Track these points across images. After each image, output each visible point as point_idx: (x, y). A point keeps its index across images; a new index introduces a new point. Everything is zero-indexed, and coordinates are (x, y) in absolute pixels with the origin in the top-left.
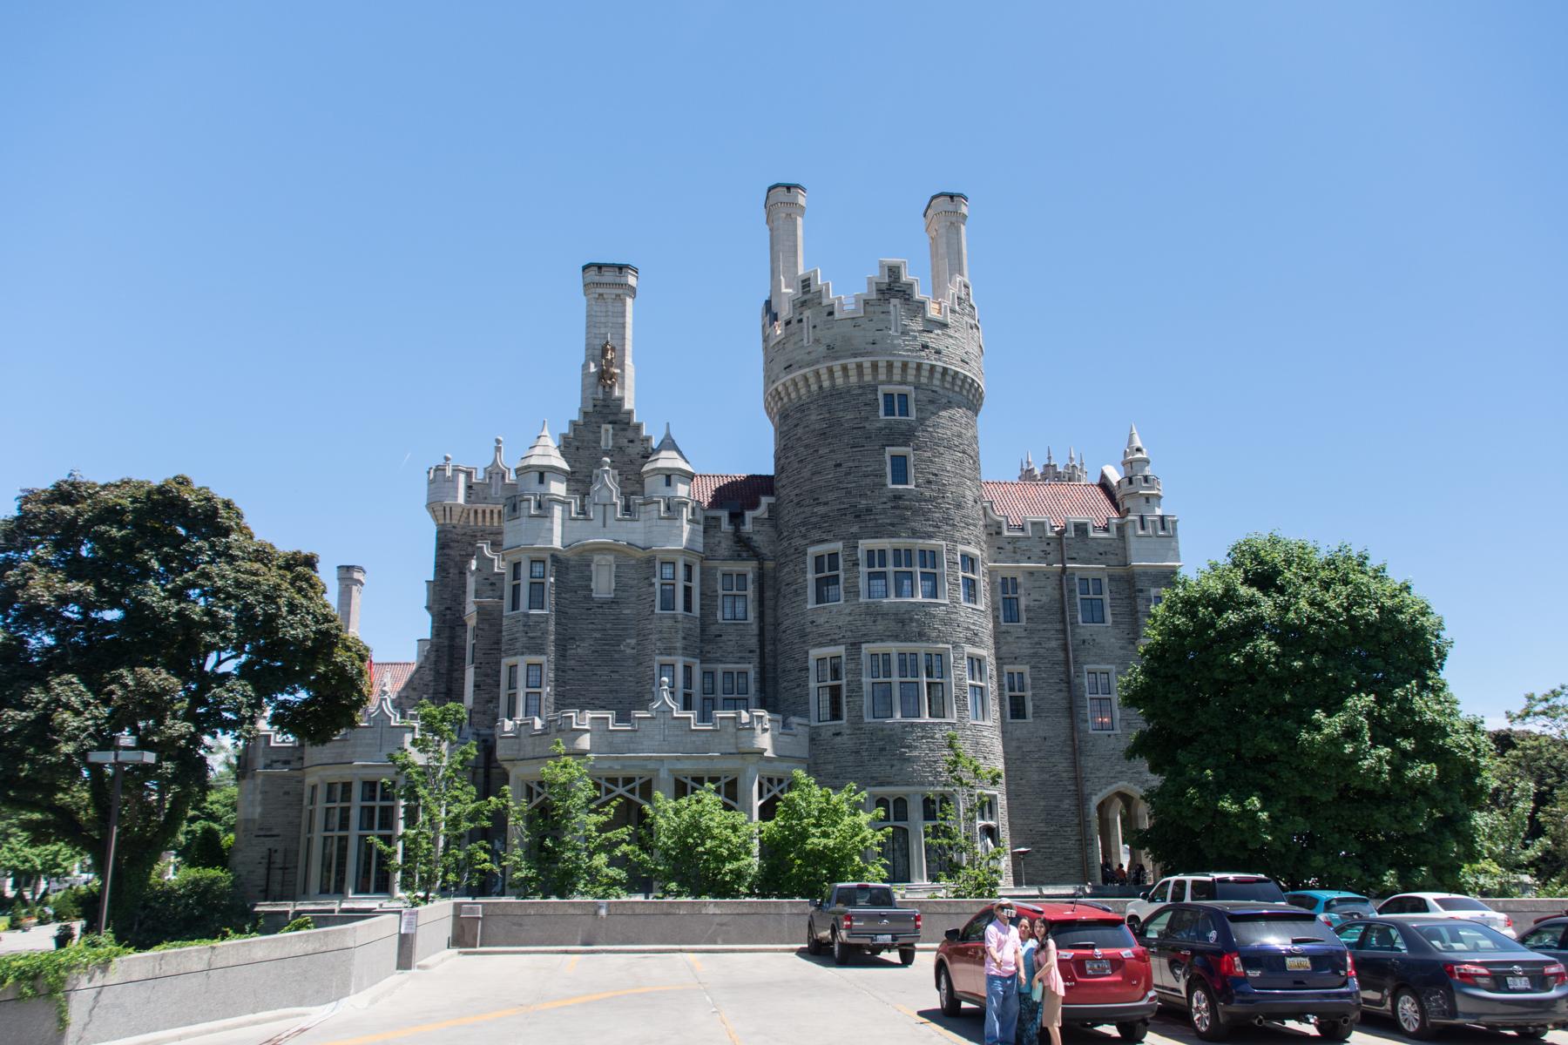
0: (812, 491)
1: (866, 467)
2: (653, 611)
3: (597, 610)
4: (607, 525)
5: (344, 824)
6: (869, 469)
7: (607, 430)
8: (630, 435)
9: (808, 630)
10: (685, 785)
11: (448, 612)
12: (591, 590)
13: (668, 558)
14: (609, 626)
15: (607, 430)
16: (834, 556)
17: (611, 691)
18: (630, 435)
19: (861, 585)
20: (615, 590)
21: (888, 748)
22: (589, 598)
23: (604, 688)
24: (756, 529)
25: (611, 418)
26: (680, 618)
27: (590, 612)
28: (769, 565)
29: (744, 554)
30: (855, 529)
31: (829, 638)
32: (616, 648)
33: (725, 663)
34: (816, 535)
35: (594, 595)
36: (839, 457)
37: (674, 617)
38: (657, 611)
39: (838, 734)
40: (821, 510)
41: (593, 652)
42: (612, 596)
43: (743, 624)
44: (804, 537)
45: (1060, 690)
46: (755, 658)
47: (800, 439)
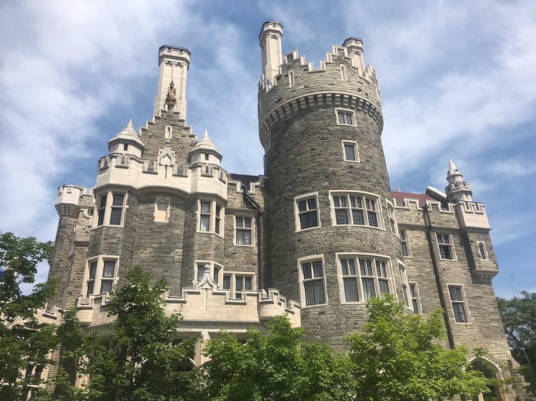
0: (296, 165)
4: (167, 177)
6: (278, 213)
7: (169, 129)
11: (61, 262)
14: (164, 240)
16: (312, 201)
19: (332, 216)
21: (359, 322)
30: (326, 184)
32: (169, 255)
36: (313, 145)
39: (323, 313)
43: (249, 248)
45: (436, 297)
46: (256, 268)
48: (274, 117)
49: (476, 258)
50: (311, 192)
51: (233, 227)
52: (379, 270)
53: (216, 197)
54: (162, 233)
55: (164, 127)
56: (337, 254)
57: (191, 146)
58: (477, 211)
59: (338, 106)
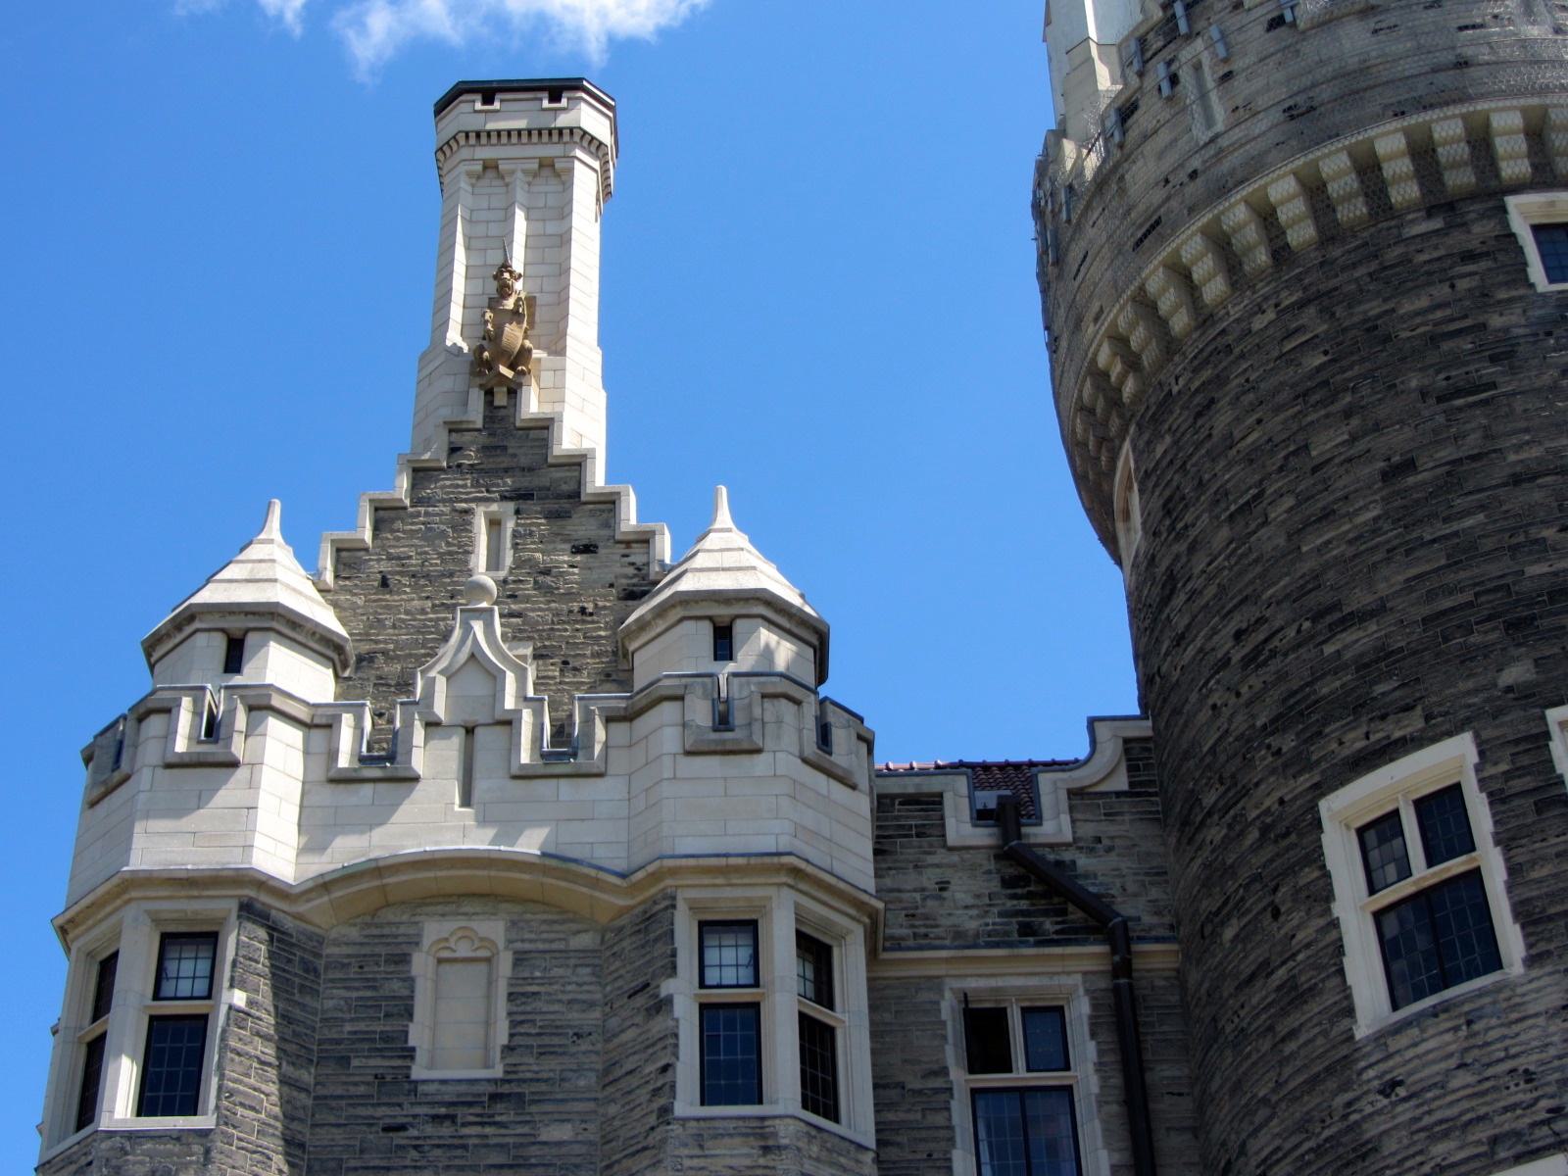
1: (1518, 448)
2: (665, 1111)
7: (494, 524)
8: (583, 528)
9: (1371, 1131)
12: (410, 1053)
13: (730, 900)
18: (583, 528)
20: (508, 1049)
22: (398, 1083)
24: (1088, 830)
26: (786, 1133)
27: (399, 1138)
28: (1156, 958)
29: (1049, 925)
30: (1516, 673)
31: (1483, 1133)
35: (418, 1072)
36: (1398, 440)
37: (762, 1136)
38: (687, 1102)
40: (1358, 640)
42: (498, 1072)
44: (1298, 763)
47: (1230, 442)
48: (1134, 345)
51: (944, 1071)
55: (466, 512)
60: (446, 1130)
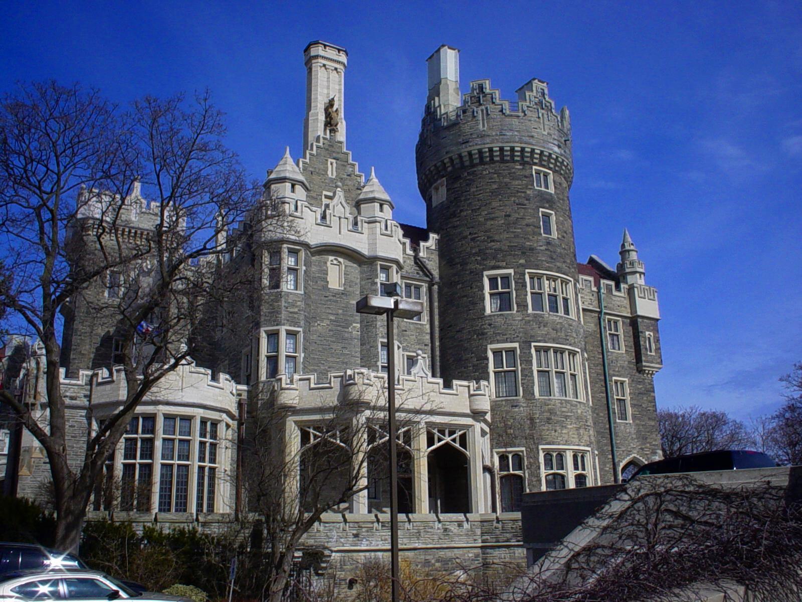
3: (332, 298)
4: (342, 233)
5: (148, 452)
7: (332, 164)
10: (433, 434)
14: (340, 311)
15: (332, 164)
16: (506, 279)
17: (343, 363)
23: (338, 360)
25: (335, 155)
30: (522, 261)
32: (347, 330)
33: (409, 352)
34: (493, 263)
36: (508, 210)
41: (330, 330)
49: (643, 351)
50: (505, 268)
52: (556, 361)
53: (396, 262)
54: (336, 302)
56: (533, 344)
57: (358, 189)
58: (650, 297)
59: (535, 164)
60: (335, 298)
